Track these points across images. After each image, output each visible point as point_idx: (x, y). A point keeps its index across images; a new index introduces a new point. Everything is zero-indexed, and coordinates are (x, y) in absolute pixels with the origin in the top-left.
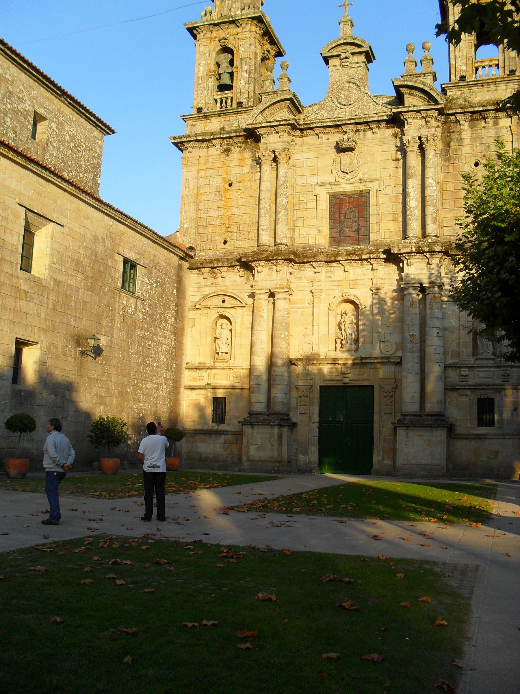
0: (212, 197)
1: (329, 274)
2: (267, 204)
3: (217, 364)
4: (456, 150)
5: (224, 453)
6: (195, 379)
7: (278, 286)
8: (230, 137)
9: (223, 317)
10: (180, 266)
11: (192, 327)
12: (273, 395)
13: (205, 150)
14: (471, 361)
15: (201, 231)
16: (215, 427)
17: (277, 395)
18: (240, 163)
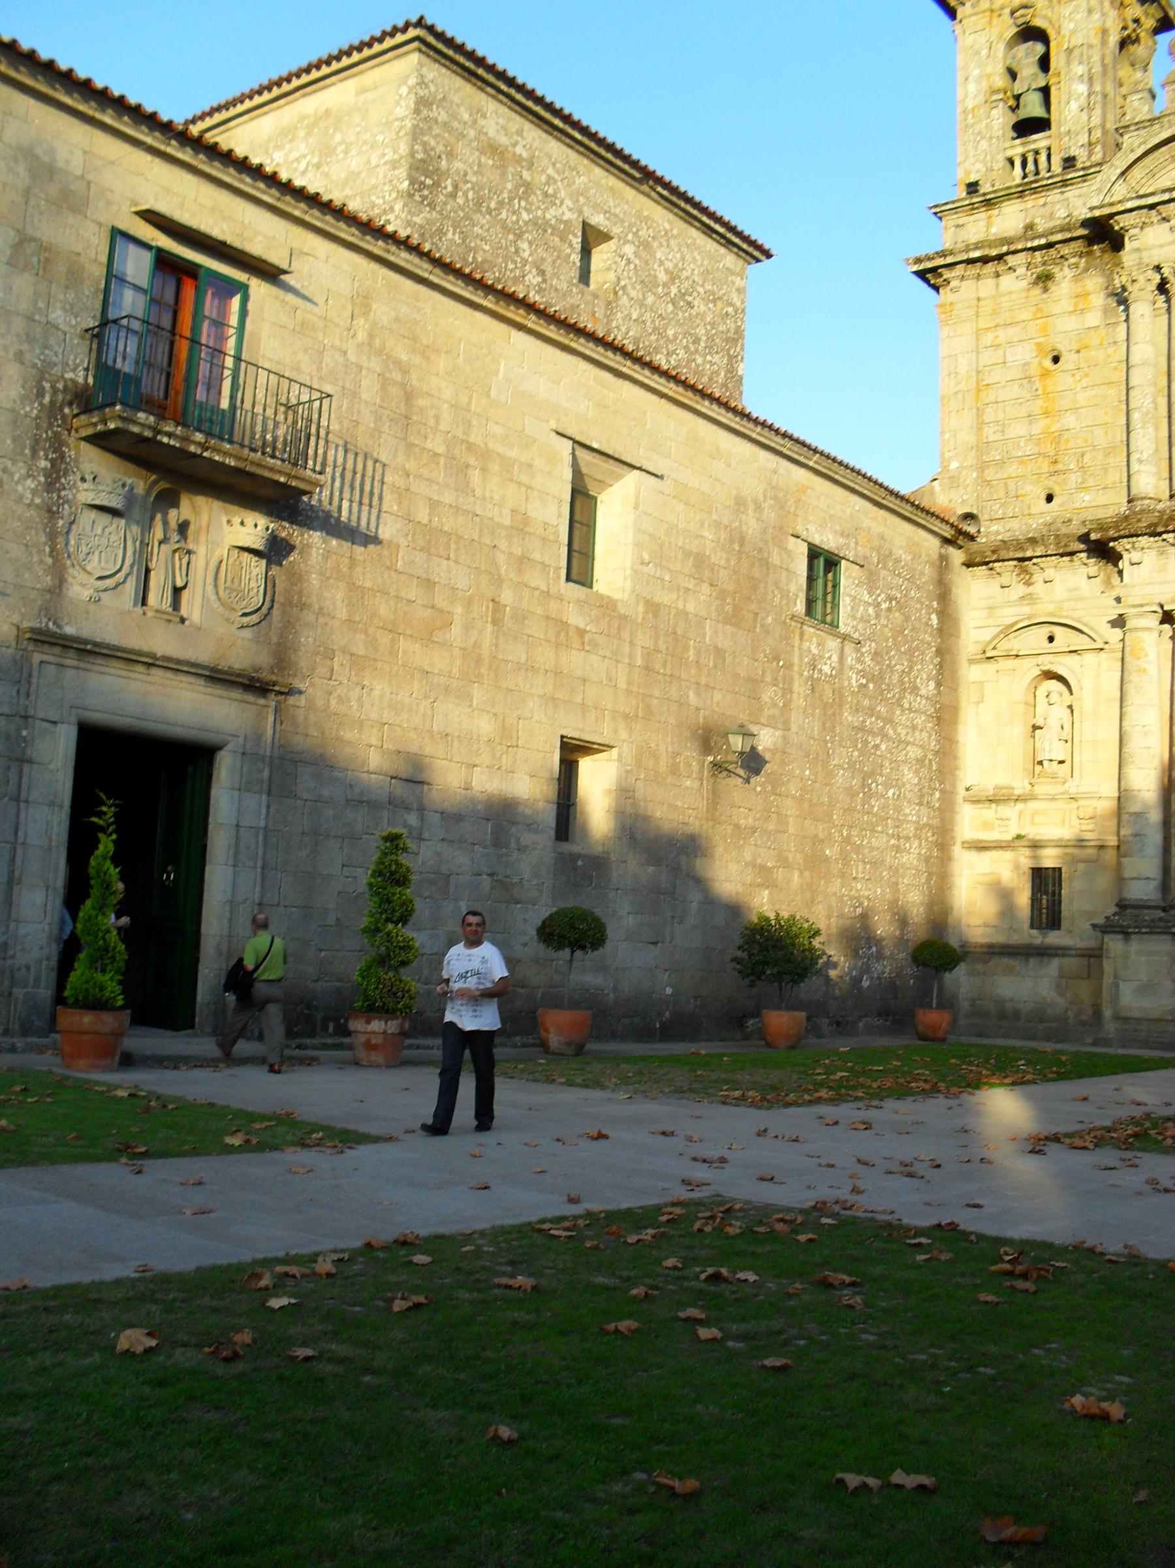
0: (1014, 391)
3: (1039, 789)
5: (1060, 1001)
6: (987, 825)
8: (1050, 246)
9: (1050, 675)
10: (943, 558)
11: (978, 703)
13: (991, 282)
15: (989, 474)
16: (1036, 938)
18: (1076, 305)
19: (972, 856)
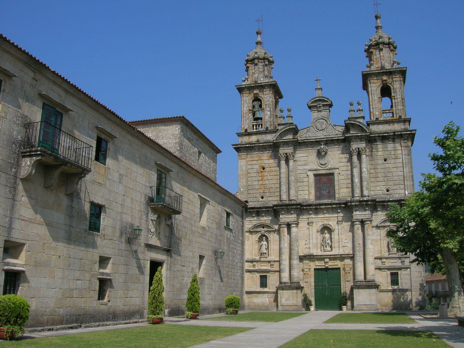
0: (255, 175)
2: (284, 180)
6: (250, 266)
7: (292, 221)
12: (292, 274)
14: (386, 255)
16: (262, 290)
17: (295, 273)
19: (248, 274)
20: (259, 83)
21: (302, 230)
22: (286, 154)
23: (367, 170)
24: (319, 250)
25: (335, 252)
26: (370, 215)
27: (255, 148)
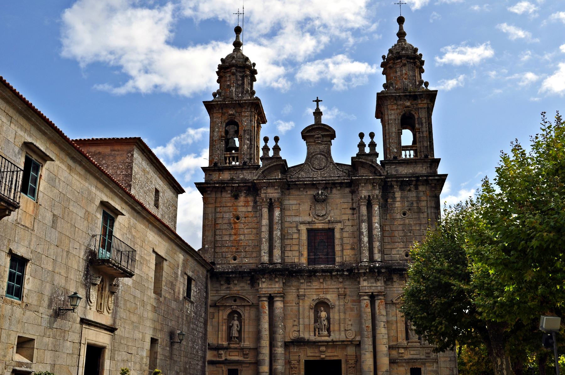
0: (226, 226)
1: (309, 284)
2: (265, 235)
4: (392, 204)
15: (217, 250)
20: (236, 101)
21: (289, 306)
22: (271, 199)
23: (380, 226)
24: (312, 334)
25: (335, 336)
26: (383, 288)
27: (227, 188)
